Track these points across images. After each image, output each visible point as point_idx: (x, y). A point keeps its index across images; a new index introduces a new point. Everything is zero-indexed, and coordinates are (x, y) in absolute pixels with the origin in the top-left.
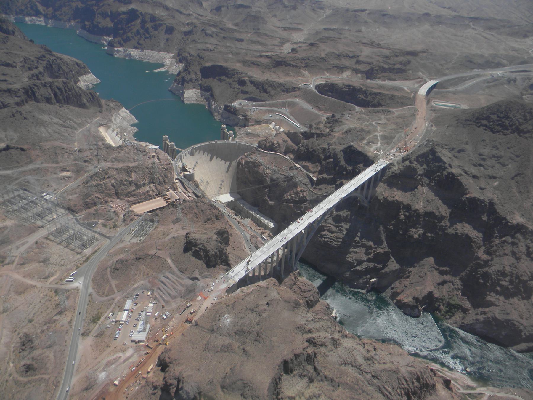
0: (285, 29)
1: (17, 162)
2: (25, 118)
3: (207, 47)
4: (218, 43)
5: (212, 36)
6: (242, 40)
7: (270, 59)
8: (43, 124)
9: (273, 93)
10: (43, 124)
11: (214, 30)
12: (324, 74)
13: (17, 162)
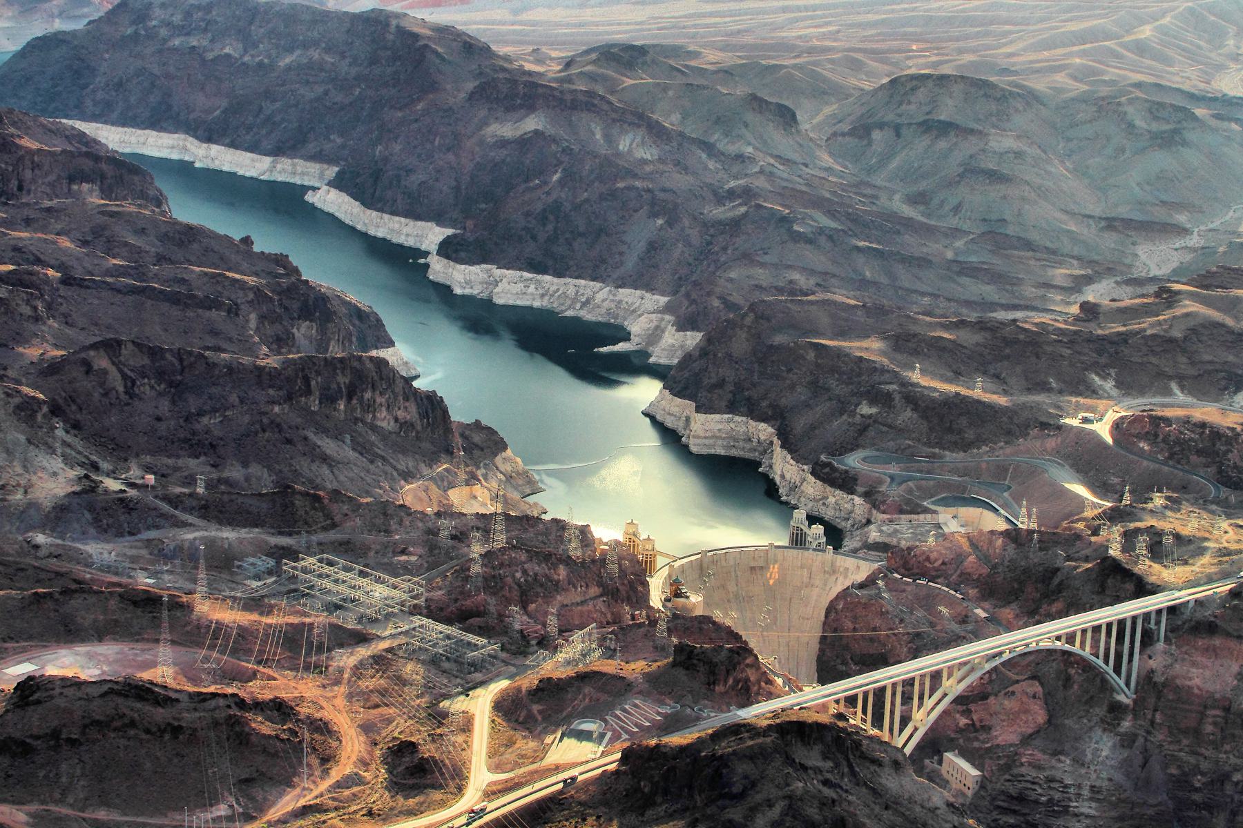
0: (1111, 224)
1: (306, 523)
2: (289, 441)
3: (791, 282)
4: (831, 268)
5: (810, 241)
6: (924, 262)
7: (988, 335)
9: (970, 435)
10: (325, 459)
11: (826, 222)
12: (1168, 392)
13: (306, 523)
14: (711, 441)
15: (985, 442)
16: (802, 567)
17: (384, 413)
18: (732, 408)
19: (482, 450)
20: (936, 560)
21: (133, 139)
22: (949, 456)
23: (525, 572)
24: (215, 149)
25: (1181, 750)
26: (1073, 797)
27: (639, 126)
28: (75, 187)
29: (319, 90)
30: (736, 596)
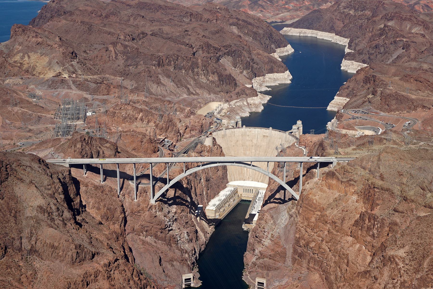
8: (159, 83)
10: (159, 83)
14: (335, 105)
15: (398, 111)
16: (280, 138)
17: (203, 77)
18: (347, 96)
19: (247, 95)
20: (309, 140)
21: (324, 35)
22: (382, 114)
23: (126, 113)
24: (338, 37)
25: (302, 227)
26: (265, 236)
27: (421, 25)
28: (231, 27)
29: (364, 20)
30: (256, 145)
